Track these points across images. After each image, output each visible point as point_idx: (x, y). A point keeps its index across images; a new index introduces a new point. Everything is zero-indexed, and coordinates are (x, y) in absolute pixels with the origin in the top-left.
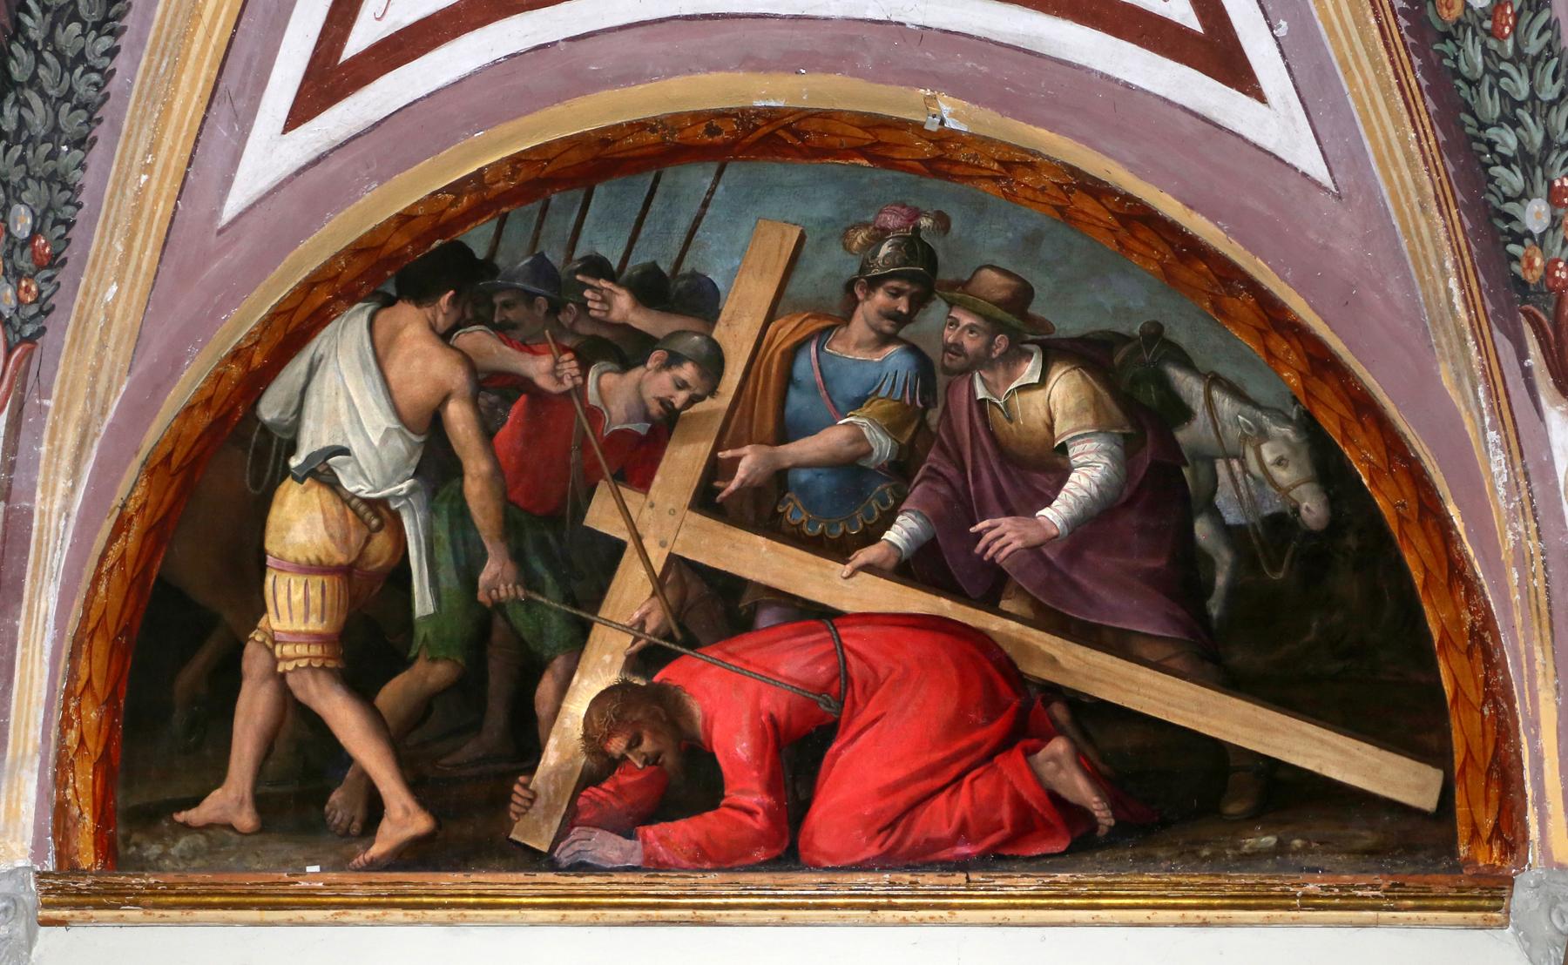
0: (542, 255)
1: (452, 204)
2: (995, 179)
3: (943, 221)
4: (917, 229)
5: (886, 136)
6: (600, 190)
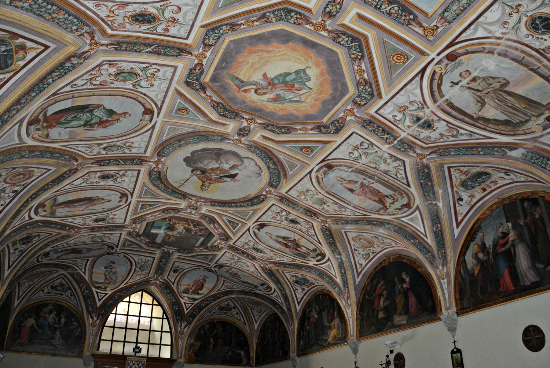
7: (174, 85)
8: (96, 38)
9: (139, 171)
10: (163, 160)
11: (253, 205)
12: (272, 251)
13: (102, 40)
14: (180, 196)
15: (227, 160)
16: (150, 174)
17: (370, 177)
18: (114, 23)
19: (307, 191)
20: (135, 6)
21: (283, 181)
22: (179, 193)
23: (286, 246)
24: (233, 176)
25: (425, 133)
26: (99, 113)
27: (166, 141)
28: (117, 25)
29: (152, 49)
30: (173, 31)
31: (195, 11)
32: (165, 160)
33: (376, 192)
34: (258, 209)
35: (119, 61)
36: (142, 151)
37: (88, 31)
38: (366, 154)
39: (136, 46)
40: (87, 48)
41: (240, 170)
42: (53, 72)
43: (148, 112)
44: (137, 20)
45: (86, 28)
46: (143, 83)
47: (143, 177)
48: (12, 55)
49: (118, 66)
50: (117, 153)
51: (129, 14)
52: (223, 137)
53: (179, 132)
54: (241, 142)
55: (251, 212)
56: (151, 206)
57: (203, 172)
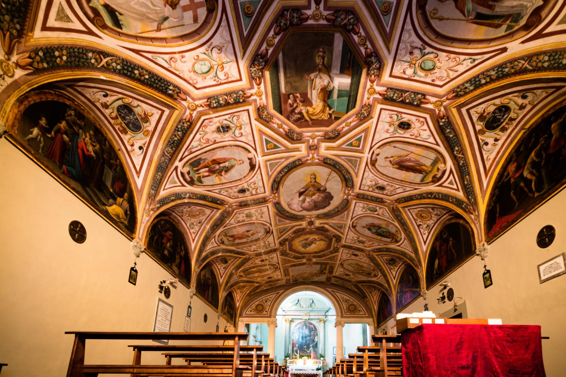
7: (345, 237)
9: (360, 189)
10: (346, 197)
11: (275, 181)
12: (215, 142)
14: (328, 162)
15: (310, 204)
16: (353, 186)
17: (251, 241)
19: (262, 217)
21: (276, 211)
22: (329, 164)
23: (215, 162)
24: (301, 194)
25: (259, 260)
26: (374, 231)
27: (345, 211)
32: (344, 196)
33: (240, 238)
34: (269, 180)
36: (358, 204)
38: (264, 246)
41: (299, 201)
43: (354, 227)
46: (356, 238)
47: (357, 181)
50: (372, 205)
52: (318, 217)
53: (339, 216)
54: (309, 218)
55: (270, 173)
56: (351, 145)
57: (319, 190)
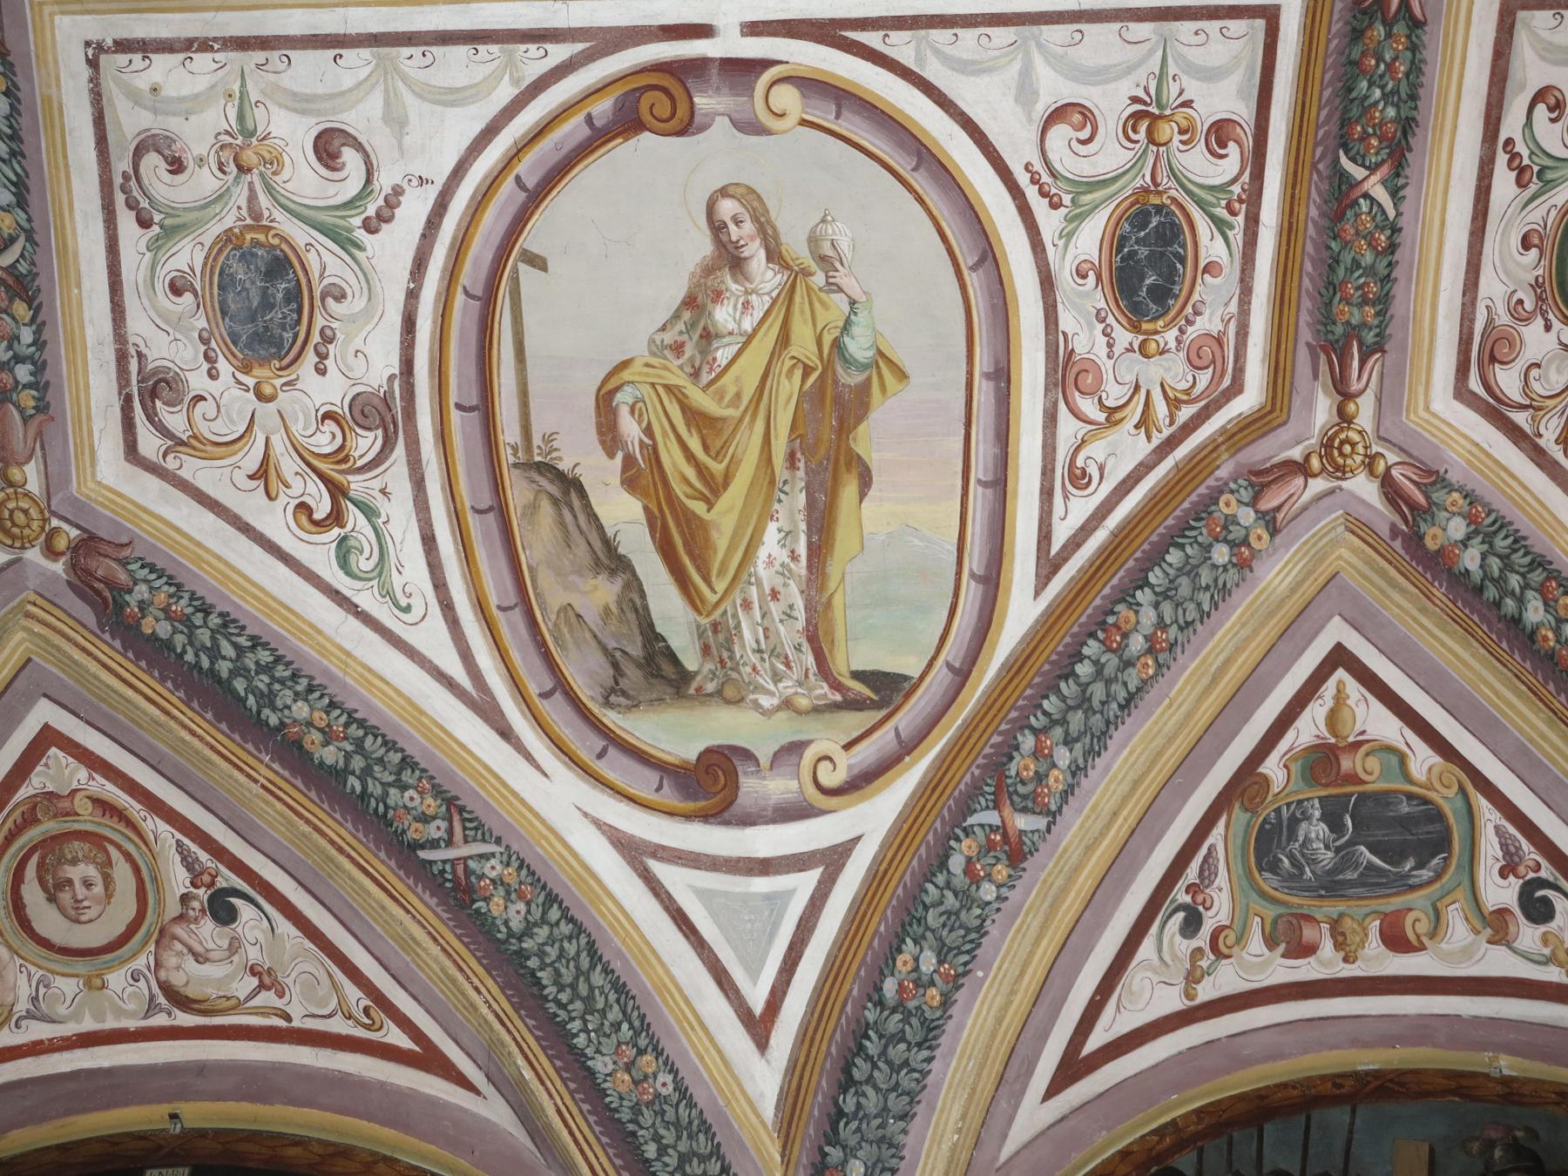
0: (1238, 1171)
1: (1158, 1143)
2: (1557, 1104)
3: (1532, 1133)
4: (1515, 1139)
5: (1464, 1082)
6: (1268, 1128)
8: (1296, 453)
13: (1309, 423)
18: (1187, 392)
20: (1067, 321)
28: (1204, 378)
29: (1372, 169)
30: (1226, 99)
31: (1056, 34)
35: (1467, 317)
37: (1246, 495)
39: (1347, 258)
40: (1364, 487)
42: (1516, 621)
44: (1162, 294)
45: (1227, 506)
48: (1363, 797)
49: (1503, 318)
51: (1123, 337)
